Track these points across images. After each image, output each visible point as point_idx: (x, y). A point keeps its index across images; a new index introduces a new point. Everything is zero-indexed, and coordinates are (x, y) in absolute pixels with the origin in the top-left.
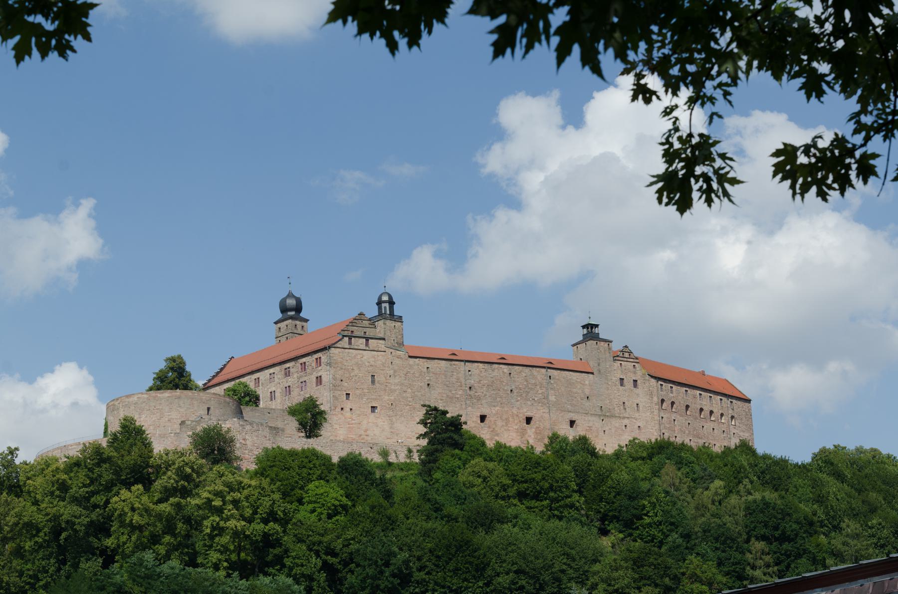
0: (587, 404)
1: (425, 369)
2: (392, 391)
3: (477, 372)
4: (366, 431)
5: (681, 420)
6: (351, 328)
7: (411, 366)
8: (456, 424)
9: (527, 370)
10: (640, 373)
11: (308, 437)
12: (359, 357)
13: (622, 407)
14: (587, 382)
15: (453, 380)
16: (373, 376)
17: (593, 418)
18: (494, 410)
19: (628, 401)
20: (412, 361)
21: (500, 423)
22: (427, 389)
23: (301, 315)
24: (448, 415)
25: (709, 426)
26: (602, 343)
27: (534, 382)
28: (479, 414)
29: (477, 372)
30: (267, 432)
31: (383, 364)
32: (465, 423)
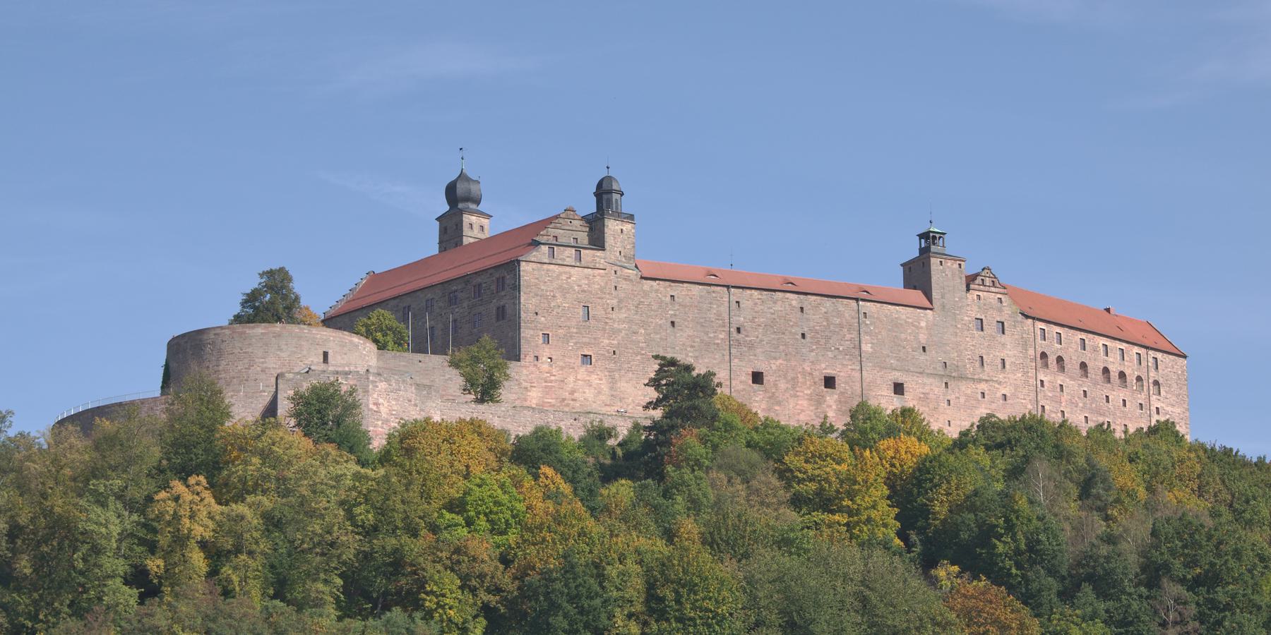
1: (668, 299)
2: (615, 332)
3: (750, 303)
4: (572, 393)
5: (1073, 385)
6: (552, 231)
7: (646, 294)
8: (704, 386)
9: (828, 303)
10: (1008, 311)
11: (481, 401)
13: (978, 364)
14: (923, 324)
15: (713, 317)
17: (931, 380)
19: (988, 354)
20: (648, 284)
21: (782, 385)
22: (670, 329)
23: (481, 208)
24: (694, 373)
25: (1118, 395)
26: (949, 263)
28: (750, 371)
29: (750, 303)
30: (411, 393)
31: (601, 290)
32: (719, 385)
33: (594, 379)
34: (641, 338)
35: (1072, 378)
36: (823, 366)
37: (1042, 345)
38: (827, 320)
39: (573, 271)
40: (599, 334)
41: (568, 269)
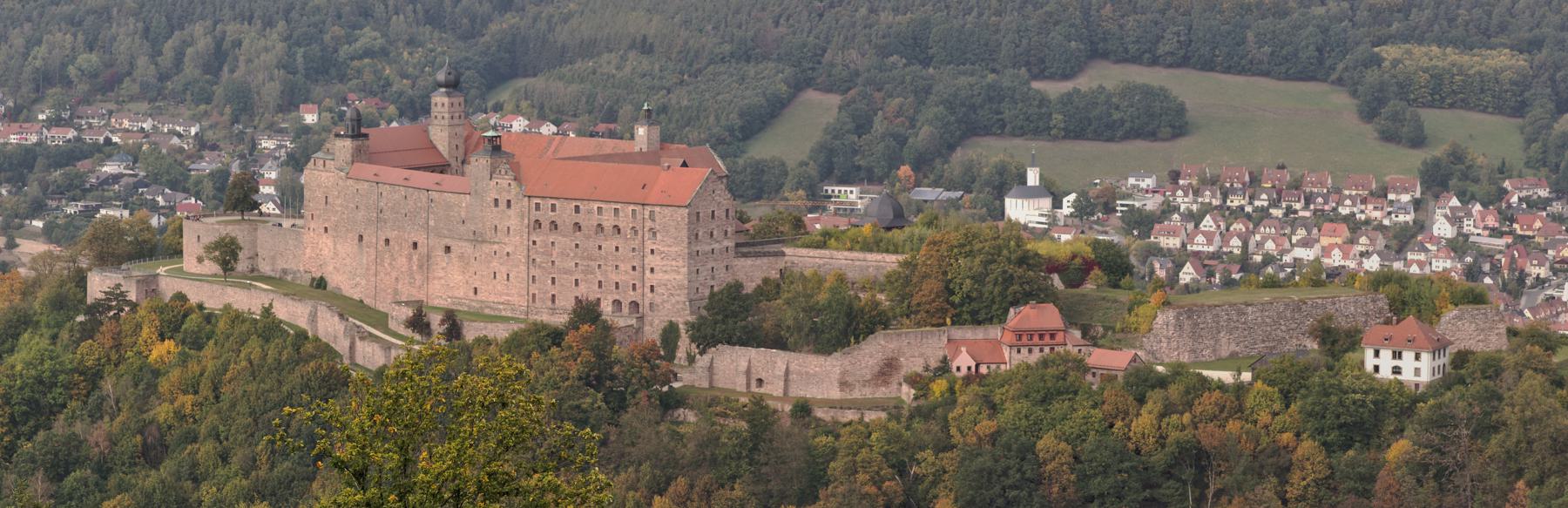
0: (462, 228)
25: (609, 245)
37: (535, 215)
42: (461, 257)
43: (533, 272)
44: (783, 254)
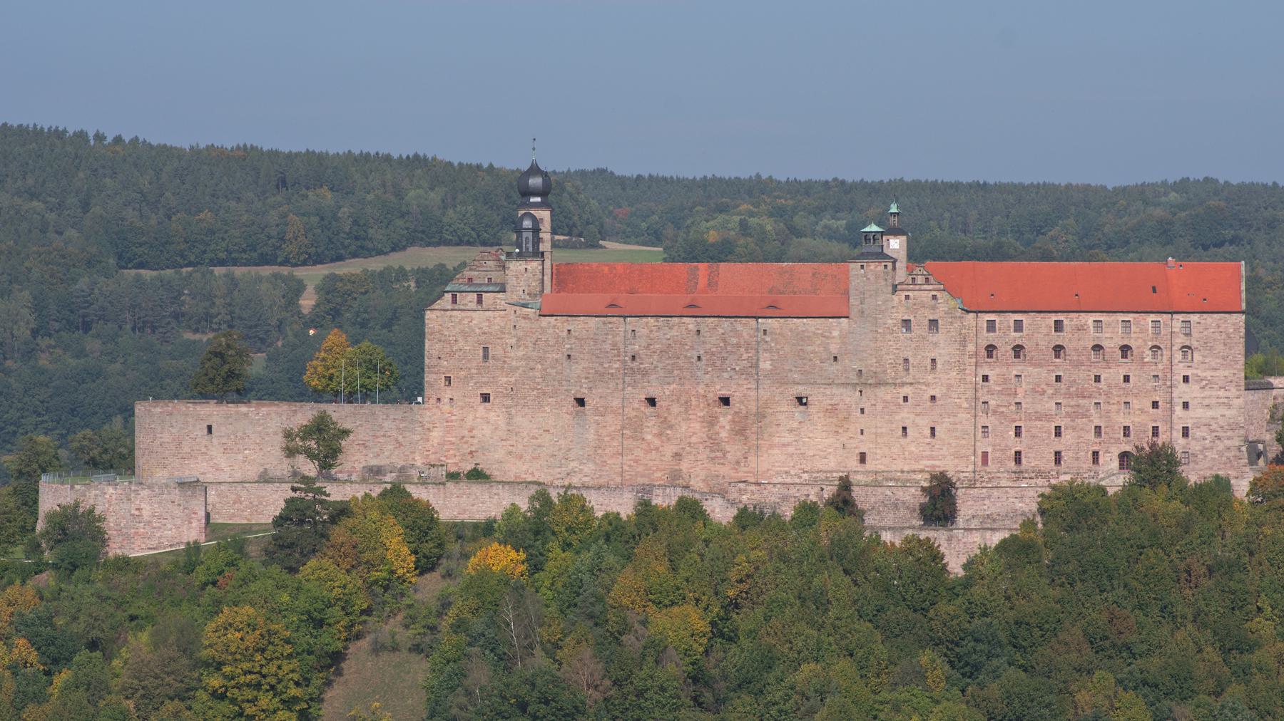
0: (833, 368)
1: (565, 333)
3: (646, 331)
7: (544, 330)
9: (726, 324)
12: (466, 322)
13: (901, 368)
14: (836, 333)
15: (607, 346)
16: (486, 349)
17: (842, 390)
18: (668, 390)
20: (545, 321)
21: (675, 409)
22: (566, 364)
25: (1111, 375)
27: (734, 341)
33: (492, 416)
34: (538, 374)
35: (1036, 365)
36: (718, 387)
37: (986, 338)
38: (724, 341)
39: (474, 314)
40: (498, 372)
41: (469, 313)
42: (832, 410)
43: (983, 420)
44: (1270, 387)
